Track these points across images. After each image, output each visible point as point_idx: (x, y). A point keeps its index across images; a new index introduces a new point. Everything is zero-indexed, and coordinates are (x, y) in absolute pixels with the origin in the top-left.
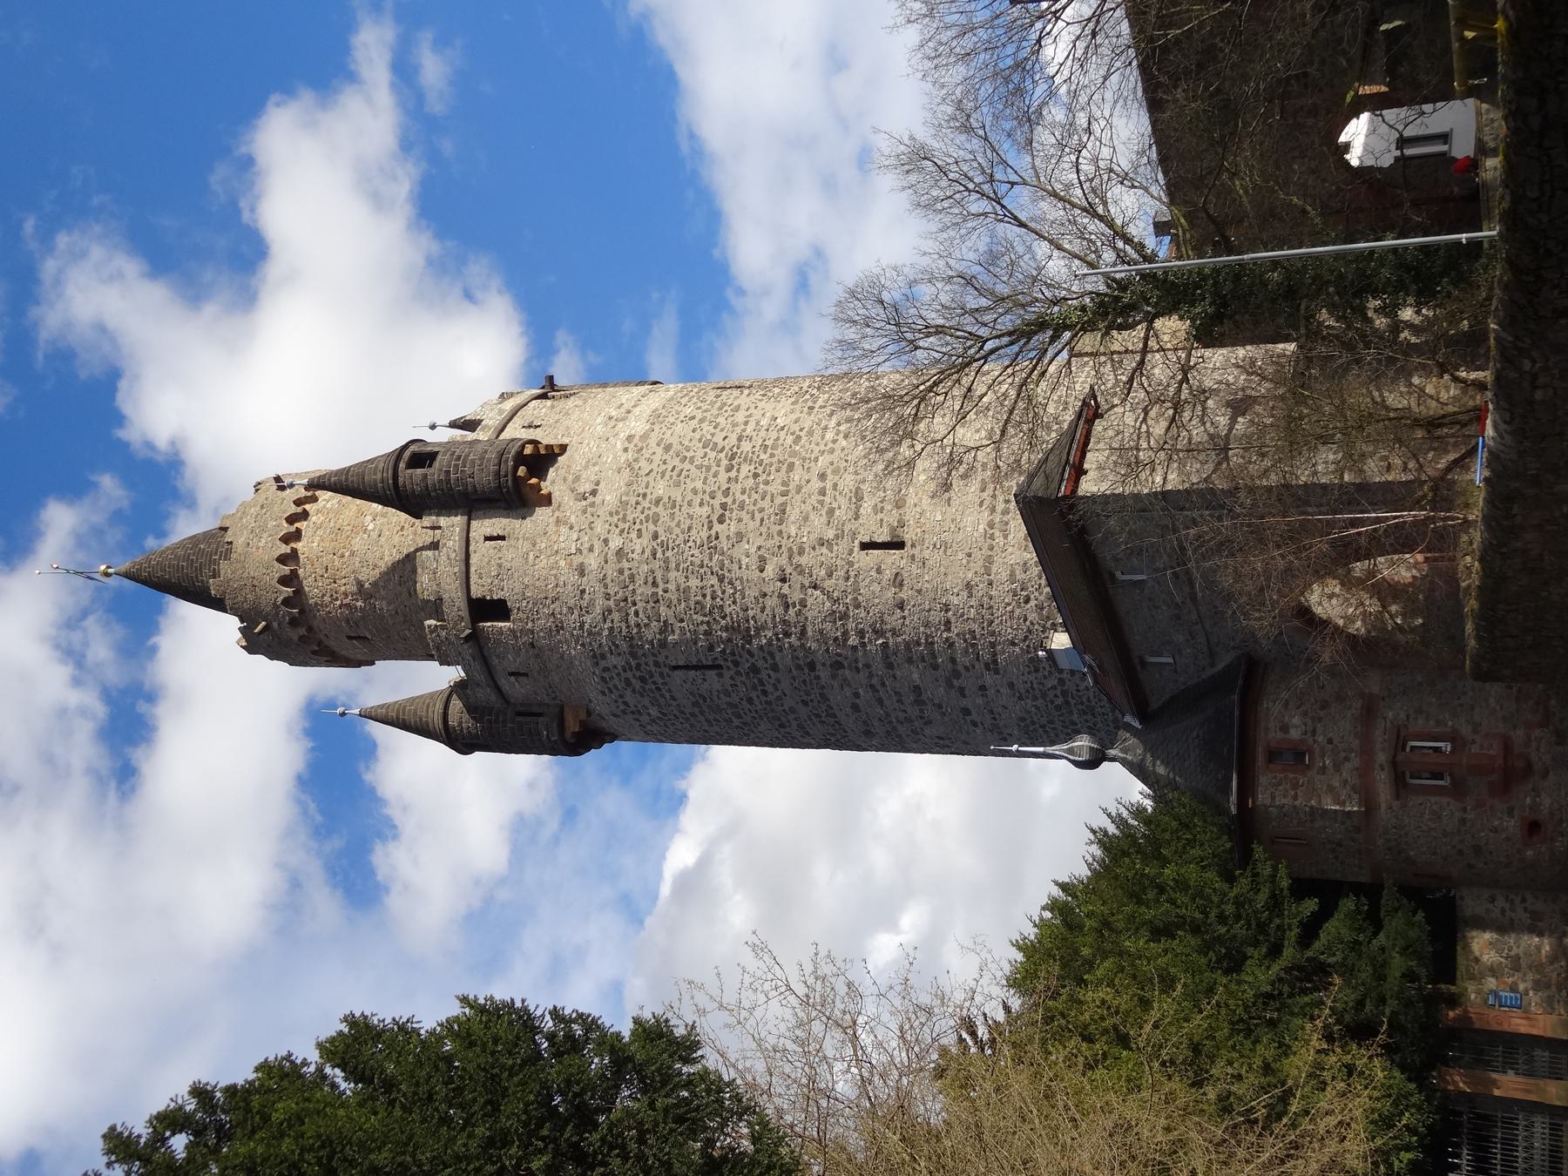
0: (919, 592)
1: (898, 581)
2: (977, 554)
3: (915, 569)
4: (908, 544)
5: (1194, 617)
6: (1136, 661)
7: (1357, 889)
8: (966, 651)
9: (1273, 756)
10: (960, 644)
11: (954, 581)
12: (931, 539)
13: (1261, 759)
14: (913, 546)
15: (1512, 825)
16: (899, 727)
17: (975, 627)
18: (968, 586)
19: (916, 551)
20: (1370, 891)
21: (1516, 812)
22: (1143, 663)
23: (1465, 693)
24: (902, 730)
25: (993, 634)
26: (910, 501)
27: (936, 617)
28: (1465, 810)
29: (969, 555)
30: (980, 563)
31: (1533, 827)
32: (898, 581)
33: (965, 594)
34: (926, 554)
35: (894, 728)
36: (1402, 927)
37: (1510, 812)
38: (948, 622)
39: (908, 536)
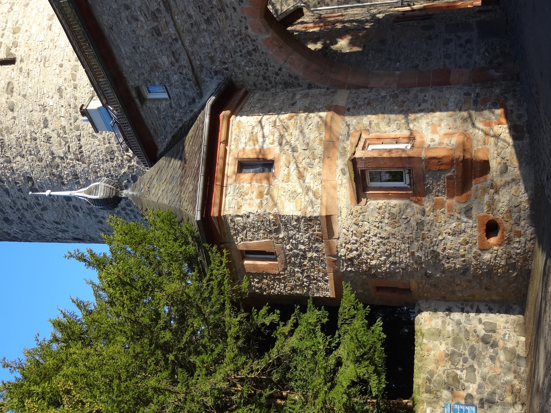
0: (24, 96)
1: (10, 89)
2: (66, 64)
3: (22, 79)
4: (18, 60)
5: (172, 30)
6: (134, 94)
7: (319, 303)
8: (60, 144)
9: (243, 165)
10: (55, 139)
11: (50, 88)
12: (34, 55)
13: (231, 169)
14: (22, 61)
15: (472, 228)
16: (25, 213)
17: (64, 122)
18: (60, 90)
19: (23, 65)
20: (331, 306)
21: (474, 213)
22: (143, 99)
23: (425, 101)
24: (28, 215)
25: (78, 128)
26: (23, 28)
27: (37, 116)
28: (423, 213)
29: (61, 66)
30: (69, 72)
31: (491, 228)
32: (10, 89)
33: (57, 96)
34: (31, 66)
35: (23, 215)
36: (359, 333)
37: (468, 212)
38: (46, 121)
39: (18, 53)
